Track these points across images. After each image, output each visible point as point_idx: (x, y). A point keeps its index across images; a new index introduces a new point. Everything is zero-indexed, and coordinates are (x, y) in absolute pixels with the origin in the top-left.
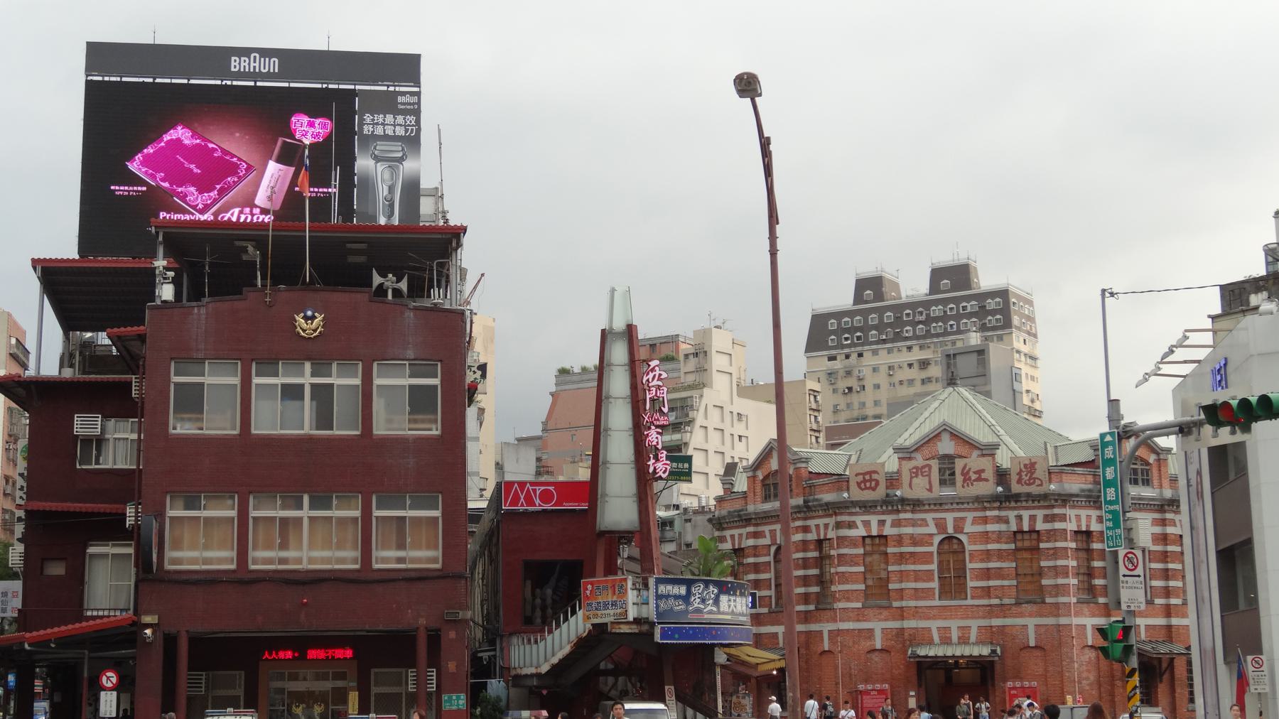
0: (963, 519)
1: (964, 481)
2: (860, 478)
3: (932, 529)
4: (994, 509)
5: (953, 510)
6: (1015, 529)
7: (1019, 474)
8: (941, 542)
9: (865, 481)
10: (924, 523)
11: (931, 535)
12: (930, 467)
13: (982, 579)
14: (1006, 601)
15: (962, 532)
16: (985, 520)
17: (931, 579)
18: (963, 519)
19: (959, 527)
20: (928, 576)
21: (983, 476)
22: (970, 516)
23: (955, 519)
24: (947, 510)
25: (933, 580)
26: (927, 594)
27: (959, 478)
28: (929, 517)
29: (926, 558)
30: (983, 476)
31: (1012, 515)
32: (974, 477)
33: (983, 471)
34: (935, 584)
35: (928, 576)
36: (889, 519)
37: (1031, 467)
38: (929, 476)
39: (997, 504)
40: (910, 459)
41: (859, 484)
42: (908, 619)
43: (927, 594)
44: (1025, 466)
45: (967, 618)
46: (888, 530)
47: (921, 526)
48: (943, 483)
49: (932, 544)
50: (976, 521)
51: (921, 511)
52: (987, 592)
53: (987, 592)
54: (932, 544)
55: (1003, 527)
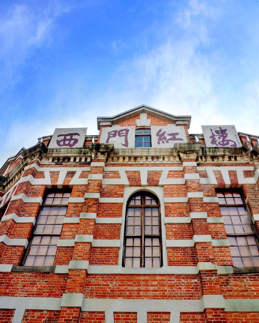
0: (158, 174)
1: (160, 140)
2: (62, 138)
3: (124, 180)
4: (191, 160)
5: (148, 165)
6: (214, 181)
7: (213, 136)
8: (132, 197)
9: (65, 140)
10: (116, 175)
11: (122, 187)
12: (127, 131)
13: (183, 238)
14: (221, 270)
15: (156, 185)
16: (182, 173)
17: (115, 236)
18: (158, 174)
19: (153, 182)
20: (112, 231)
21: (177, 137)
22: (165, 170)
23: (149, 173)
24: (142, 165)
25: (118, 237)
26: (107, 256)
27: (155, 139)
28: (122, 170)
29: (113, 210)
30: (177, 137)
31: (210, 170)
32: (168, 137)
33: (177, 134)
34: (118, 243)
35: (112, 231)
36: (79, 170)
37: (222, 132)
38: (126, 136)
39: (193, 156)
40: (111, 126)
41: (58, 142)
42: (72, 290)
43: (107, 256)
44: (217, 132)
45: (164, 297)
46: (75, 181)
47: (112, 177)
48: (138, 144)
49: (122, 196)
50: (171, 175)
51: (114, 165)
52: (192, 255)
53: (192, 255)
54: (122, 196)
55: (203, 181)
